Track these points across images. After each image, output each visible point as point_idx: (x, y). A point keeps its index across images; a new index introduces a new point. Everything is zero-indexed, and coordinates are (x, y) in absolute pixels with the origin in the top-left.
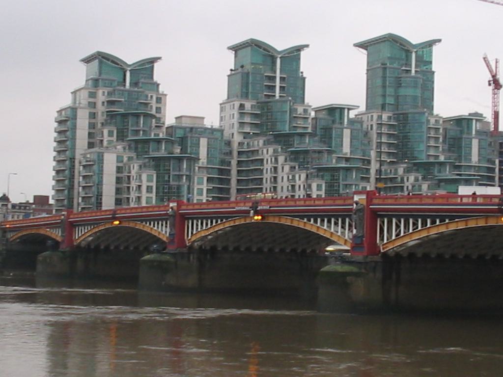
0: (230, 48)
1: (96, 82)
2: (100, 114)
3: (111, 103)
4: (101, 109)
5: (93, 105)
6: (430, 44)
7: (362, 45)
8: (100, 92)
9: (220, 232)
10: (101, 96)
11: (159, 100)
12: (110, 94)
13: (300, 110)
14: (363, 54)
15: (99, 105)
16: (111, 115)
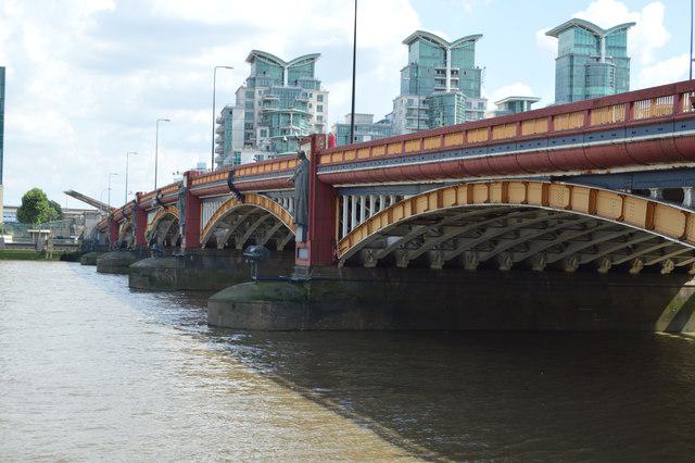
0: (404, 42)
1: (252, 80)
2: (256, 114)
3: (266, 101)
4: (258, 109)
5: (250, 106)
6: (624, 28)
7: (555, 33)
8: (257, 92)
9: (392, 240)
10: (258, 97)
11: (320, 98)
12: (269, 91)
13: (475, 104)
14: (554, 41)
15: (256, 104)
16: (266, 114)
